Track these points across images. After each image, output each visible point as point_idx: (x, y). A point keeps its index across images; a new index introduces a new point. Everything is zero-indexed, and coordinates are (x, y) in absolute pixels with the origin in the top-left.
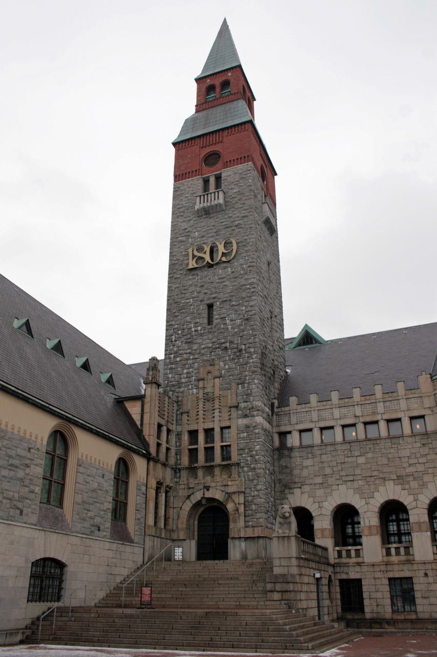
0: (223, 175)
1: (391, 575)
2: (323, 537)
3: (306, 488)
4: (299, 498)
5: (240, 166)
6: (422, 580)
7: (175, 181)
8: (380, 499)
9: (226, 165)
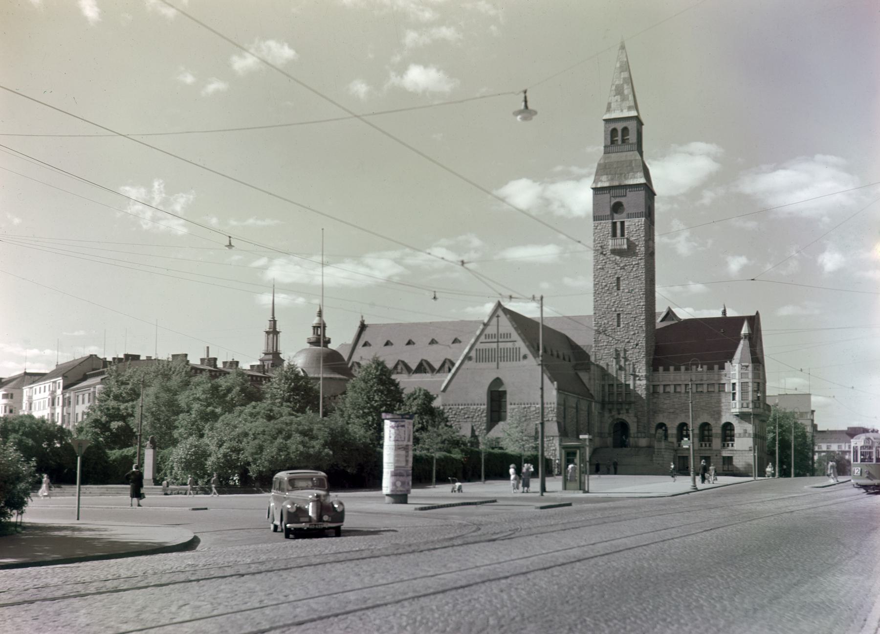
0: (626, 224)
1: (701, 455)
2: (672, 437)
3: (665, 414)
4: (661, 419)
5: (637, 220)
6: (715, 457)
7: (594, 220)
8: (700, 421)
9: (629, 216)
